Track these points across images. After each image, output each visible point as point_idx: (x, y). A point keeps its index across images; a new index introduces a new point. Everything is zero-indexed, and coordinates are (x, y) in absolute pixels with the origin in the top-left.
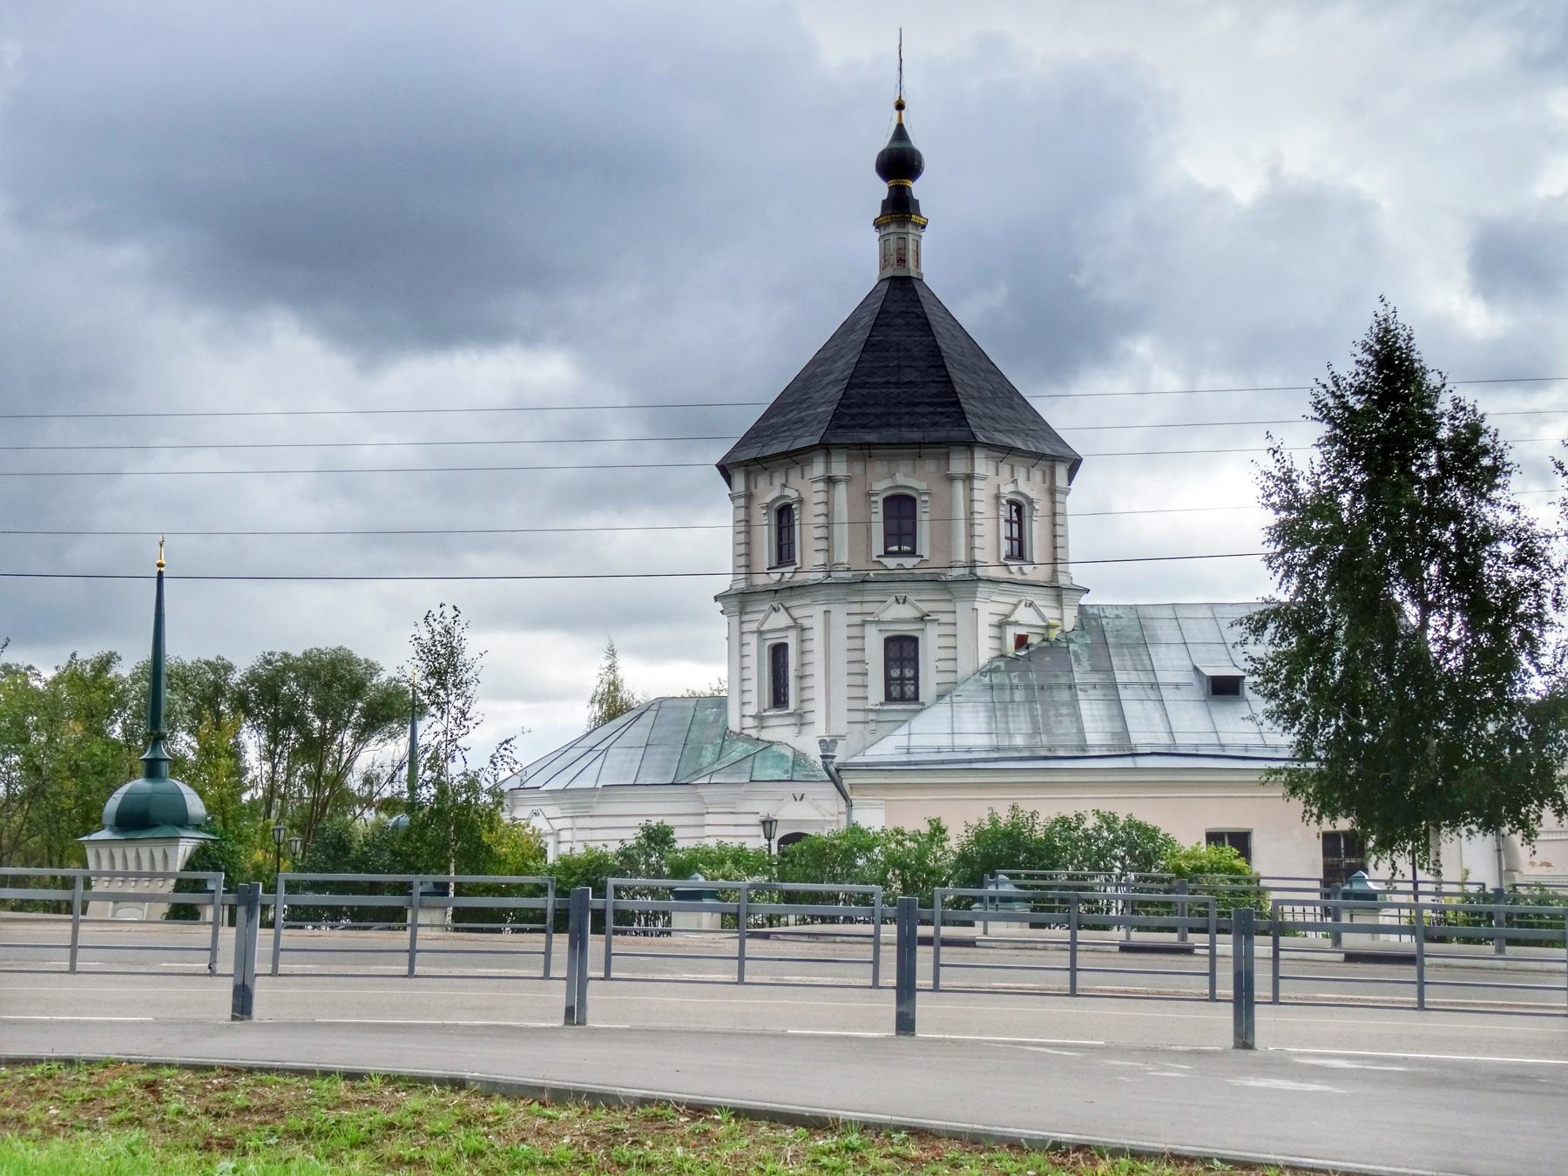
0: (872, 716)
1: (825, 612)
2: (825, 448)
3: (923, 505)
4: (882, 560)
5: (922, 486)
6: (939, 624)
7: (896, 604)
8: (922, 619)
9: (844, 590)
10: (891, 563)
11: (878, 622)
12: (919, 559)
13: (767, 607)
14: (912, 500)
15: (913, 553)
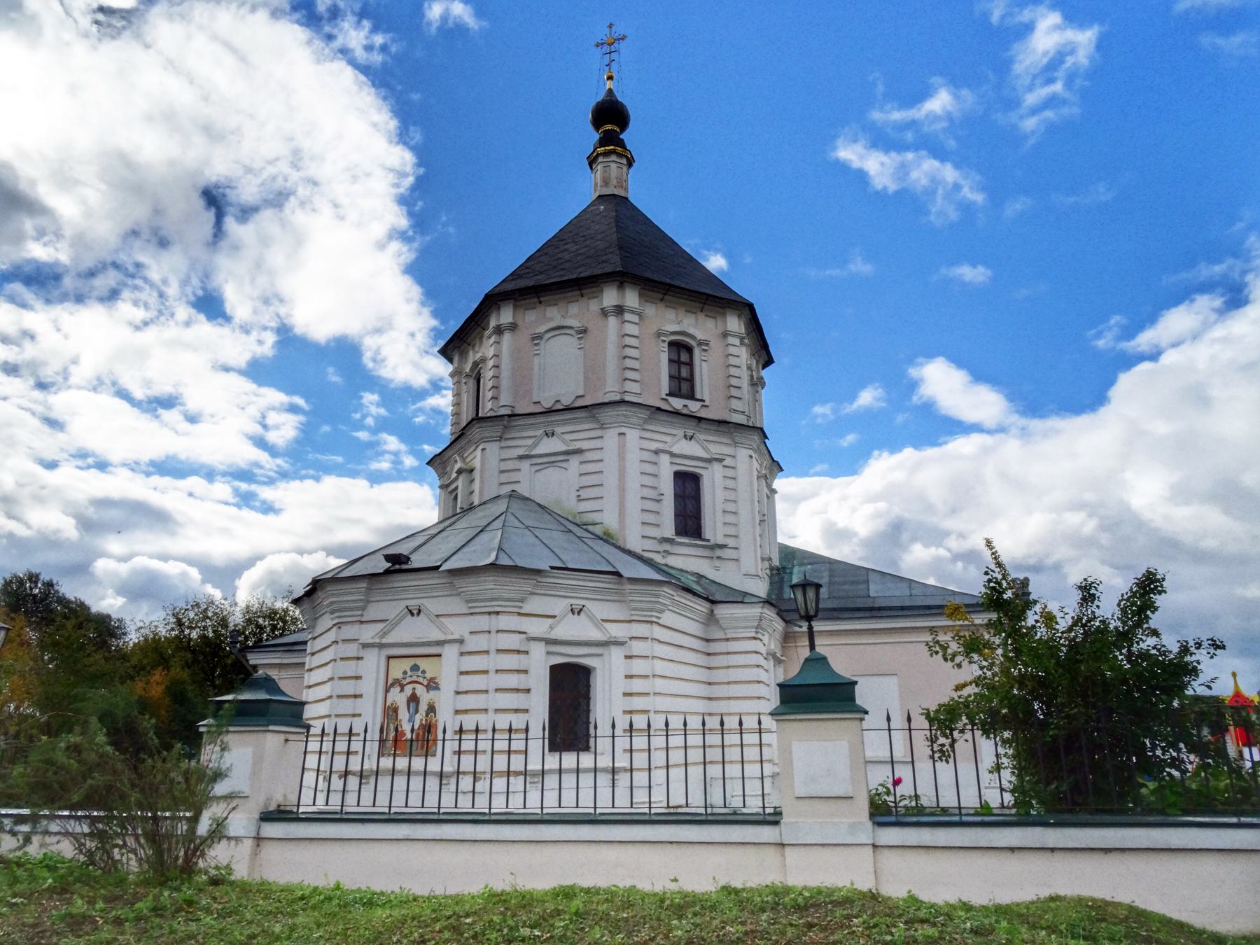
0: (667, 547)
1: (620, 434)
2: (622, 278)
3: (703, 354)
4: (669, 398)
5: (700, 336)
6: (724, 466)
7: (684, 440)
8: (709, 461)
9: (644, 414)
10: (677, 403)
11: (672, 455)
12: (700, 404)
13: (540, 432)
14: (689, 350)
15: (691, 396)
